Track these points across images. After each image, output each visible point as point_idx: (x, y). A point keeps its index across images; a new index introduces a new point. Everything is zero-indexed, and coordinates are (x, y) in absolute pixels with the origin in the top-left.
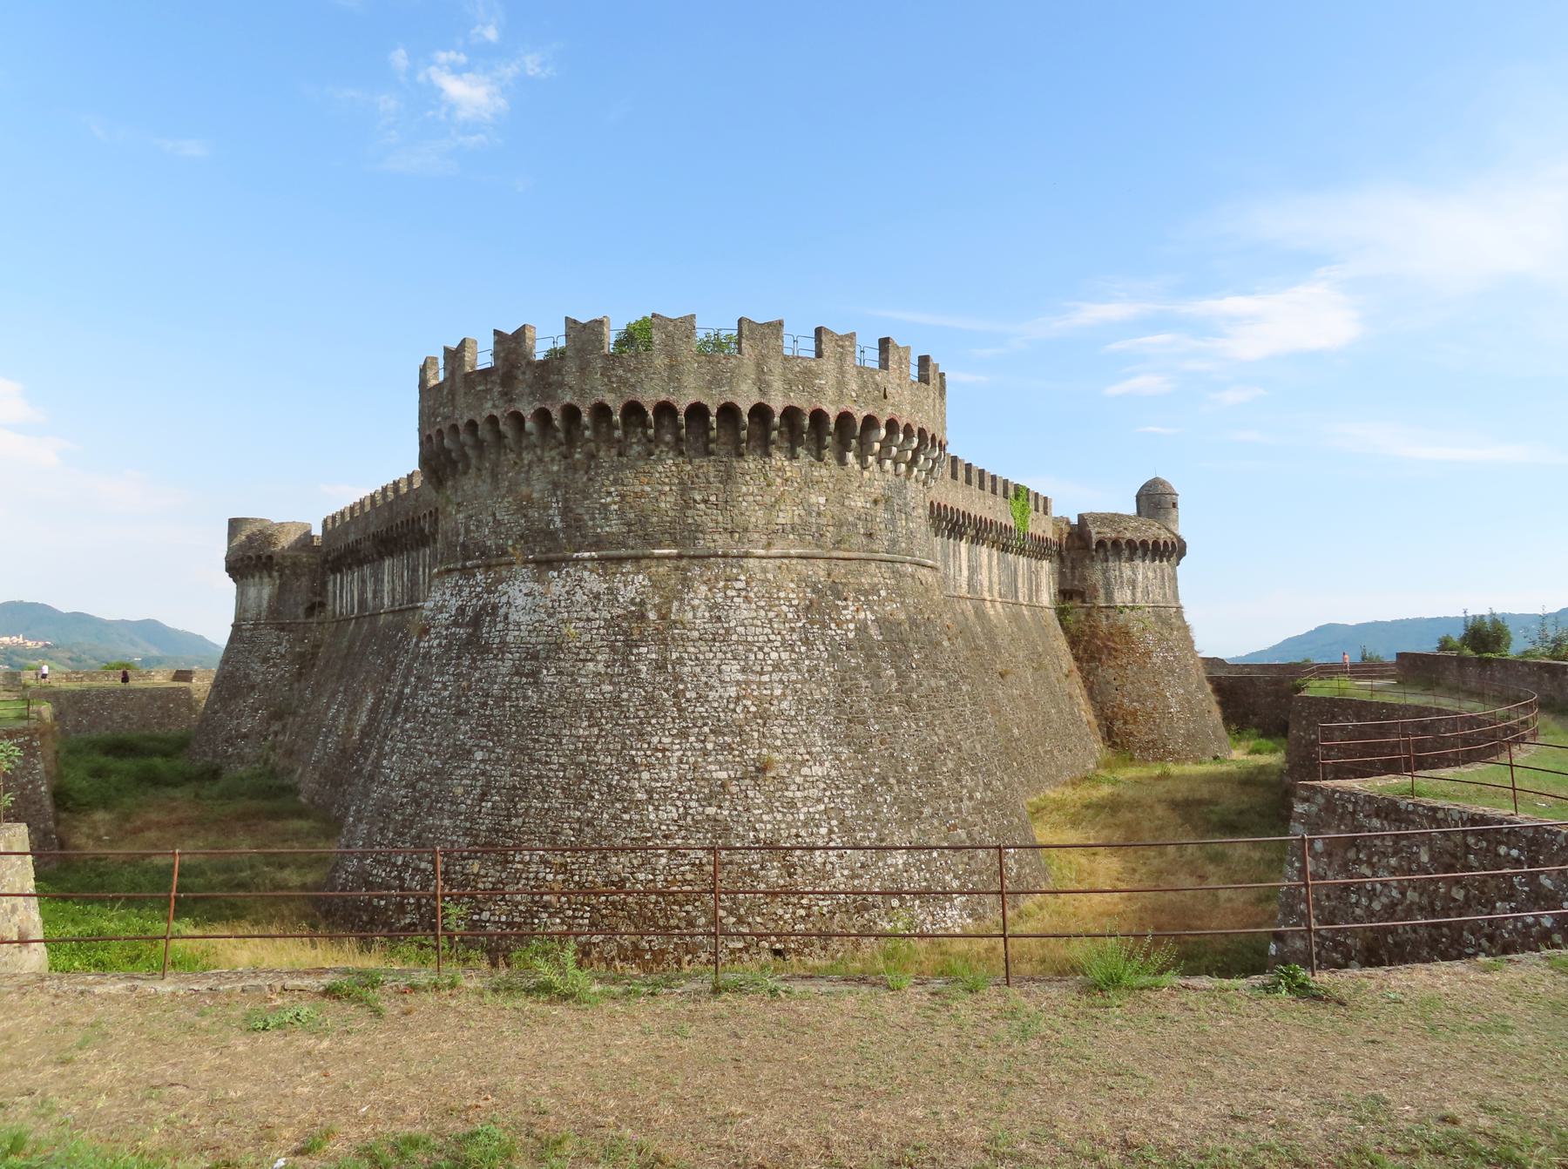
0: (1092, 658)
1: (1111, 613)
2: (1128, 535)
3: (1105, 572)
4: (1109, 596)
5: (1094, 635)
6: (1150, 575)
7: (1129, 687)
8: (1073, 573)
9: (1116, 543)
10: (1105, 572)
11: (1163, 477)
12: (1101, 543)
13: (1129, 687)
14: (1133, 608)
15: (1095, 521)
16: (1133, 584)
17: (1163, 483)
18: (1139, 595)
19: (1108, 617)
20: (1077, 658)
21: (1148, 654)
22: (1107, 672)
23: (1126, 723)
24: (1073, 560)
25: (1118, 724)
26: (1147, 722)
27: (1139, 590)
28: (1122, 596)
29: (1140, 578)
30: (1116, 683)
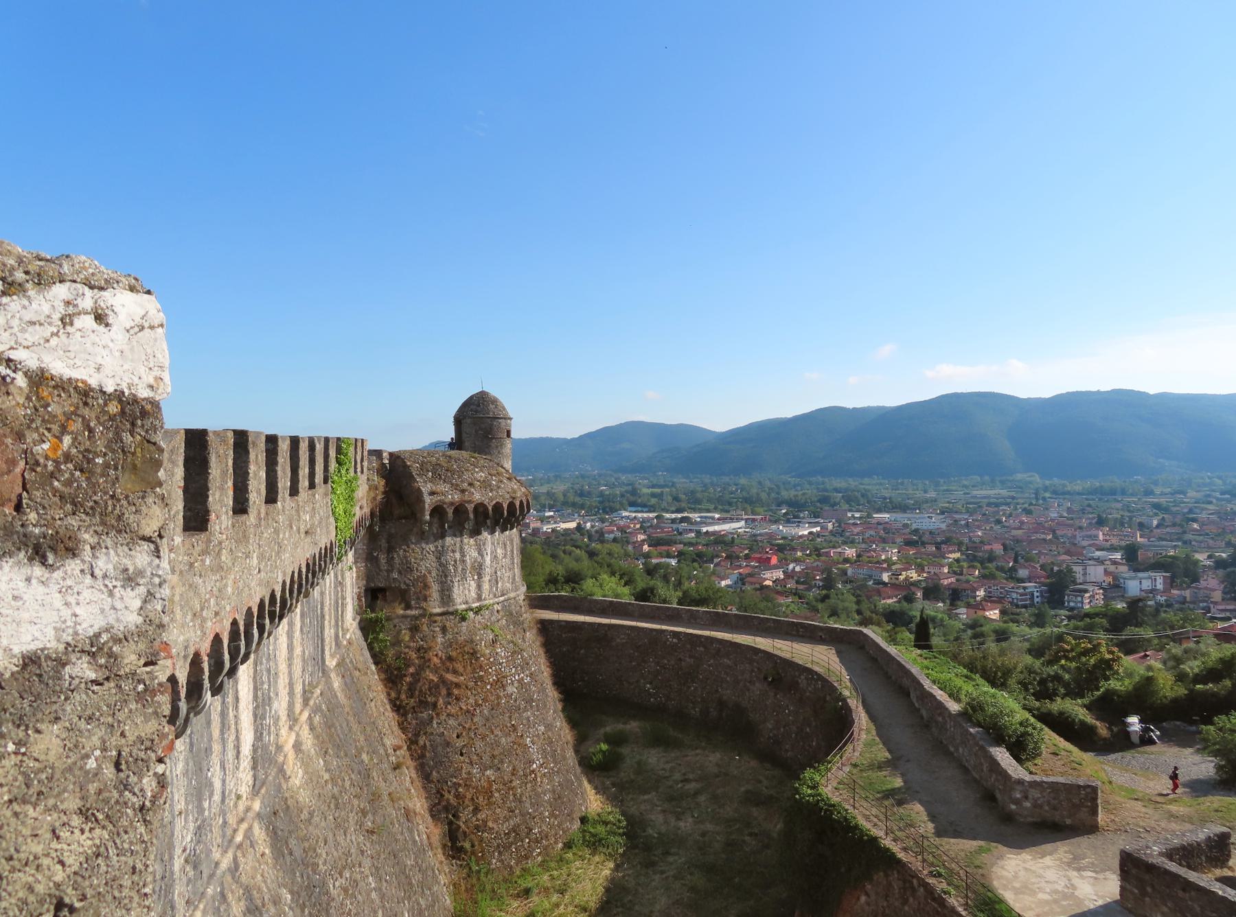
0: (423, 704)
1: (450, 622)
2: (477, 497)
3: (440, 555)
4: (446, 596)
5: (425, 663)
6: (500, 551)
7: (479, 744)
8: (390, 561)
9: (460, 510)
10: (440, 555)
11: (493, 391)
12: (438, 511)
13: (479, 744)
14: (478, 611)
15: (423, 468)
16: (478, 569)
17: (495, 401)
18: (486, 586)
19: (444, 630)
20: (397, 707)
21: (500, 683)
22: (446, 725)
23: (476, 810)
24: (390, 538)
25: (465, 814)
26: (504, 799)
27: (486, 578)
28: (464, 593)
29: (488, 559)
30: (459, 743)
